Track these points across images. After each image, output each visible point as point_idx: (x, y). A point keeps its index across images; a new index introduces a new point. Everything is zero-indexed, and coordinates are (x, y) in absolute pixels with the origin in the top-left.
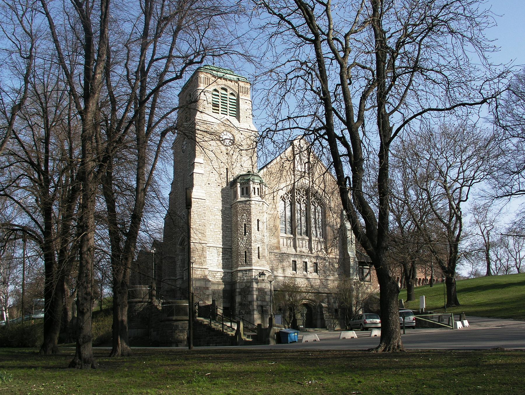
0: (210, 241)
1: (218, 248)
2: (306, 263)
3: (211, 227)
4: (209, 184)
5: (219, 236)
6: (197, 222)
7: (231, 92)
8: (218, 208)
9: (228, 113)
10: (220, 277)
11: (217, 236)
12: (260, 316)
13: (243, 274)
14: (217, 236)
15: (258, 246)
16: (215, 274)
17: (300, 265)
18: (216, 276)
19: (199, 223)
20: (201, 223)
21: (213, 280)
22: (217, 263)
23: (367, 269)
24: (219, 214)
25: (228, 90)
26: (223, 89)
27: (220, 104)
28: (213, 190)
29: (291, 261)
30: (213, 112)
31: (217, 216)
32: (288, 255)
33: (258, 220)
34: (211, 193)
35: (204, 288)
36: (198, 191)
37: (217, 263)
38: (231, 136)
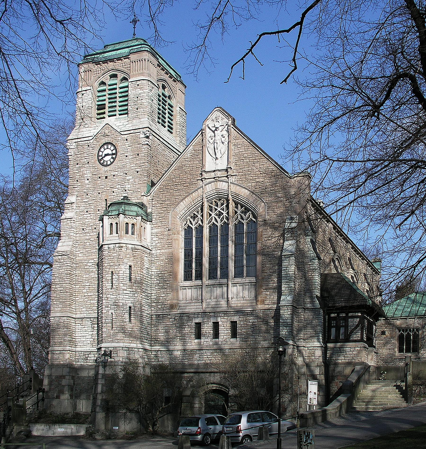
0: (83, 310)
3: (85, 291)
5: (94, 302)
7: (123, 75)
8: (93, 261)
9: (117, 113)
10: (92, 358)
11: (92, 302)
12: (104, 415)
14: (92, 302)
17: (207, 328)
21: (85, 364)
23: (357, 317)
24: (95, 270)
27: (106, 102)
29: (193, 324)
30: (98, 119)
31: (92, 274)
32: (189, 316)
35: (61, 376)
38: (112, 148)
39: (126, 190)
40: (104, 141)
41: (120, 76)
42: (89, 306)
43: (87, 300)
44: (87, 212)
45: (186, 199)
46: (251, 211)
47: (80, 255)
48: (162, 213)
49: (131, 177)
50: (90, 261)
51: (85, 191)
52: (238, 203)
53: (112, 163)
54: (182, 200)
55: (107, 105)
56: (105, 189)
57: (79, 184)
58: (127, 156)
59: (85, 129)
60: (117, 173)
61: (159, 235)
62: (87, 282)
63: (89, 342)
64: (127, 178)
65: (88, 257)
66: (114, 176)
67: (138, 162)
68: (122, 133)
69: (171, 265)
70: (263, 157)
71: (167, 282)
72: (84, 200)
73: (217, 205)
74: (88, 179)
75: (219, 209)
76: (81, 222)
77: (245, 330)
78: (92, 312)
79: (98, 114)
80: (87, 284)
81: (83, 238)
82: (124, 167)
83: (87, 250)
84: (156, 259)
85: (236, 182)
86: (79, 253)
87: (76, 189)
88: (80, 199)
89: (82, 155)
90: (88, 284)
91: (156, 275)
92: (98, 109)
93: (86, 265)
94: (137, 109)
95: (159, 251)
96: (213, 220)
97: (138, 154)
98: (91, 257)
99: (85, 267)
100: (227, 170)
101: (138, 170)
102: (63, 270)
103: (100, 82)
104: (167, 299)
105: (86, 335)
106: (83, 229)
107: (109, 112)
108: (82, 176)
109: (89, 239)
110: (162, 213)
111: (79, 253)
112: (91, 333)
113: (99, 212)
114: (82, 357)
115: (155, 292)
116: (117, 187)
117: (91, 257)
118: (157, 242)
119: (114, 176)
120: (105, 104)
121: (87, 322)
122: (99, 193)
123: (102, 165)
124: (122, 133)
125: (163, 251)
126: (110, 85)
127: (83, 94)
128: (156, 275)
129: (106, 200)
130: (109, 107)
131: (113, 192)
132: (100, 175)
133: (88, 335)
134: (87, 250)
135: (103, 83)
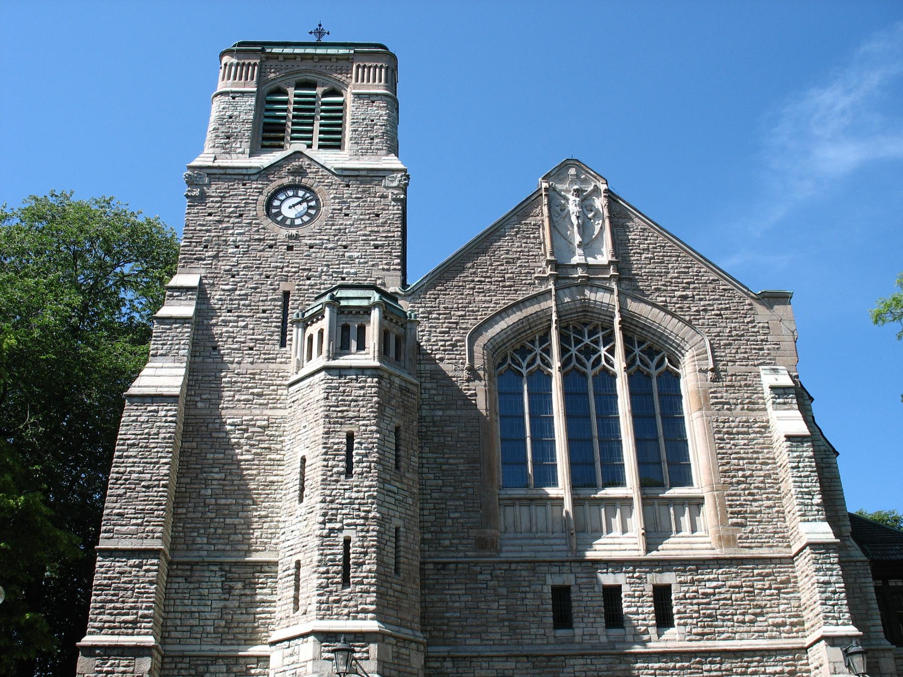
11: (228, 521)
29: (547, 589)
42: (220, 531)
43: (213, 515)
47: (200, 405)
69: (475, 447)
71: (467, 484)
73: (581, 333)
75: (587, 341)
77: (696, 607)
78: (228, 547)
79: (264, 139)
84: (432, 429)
86: (198, 399)
91: (434, 466)
92: (264, 131)
94: (372, 139)
95: (440, 413)
96: (574, 362)
97: (378, 215)
103: (273, 87)
104: (468, 525)
112: (220, 604)
115: (431, 506)
128: (434, 466)
133: (208, 609)
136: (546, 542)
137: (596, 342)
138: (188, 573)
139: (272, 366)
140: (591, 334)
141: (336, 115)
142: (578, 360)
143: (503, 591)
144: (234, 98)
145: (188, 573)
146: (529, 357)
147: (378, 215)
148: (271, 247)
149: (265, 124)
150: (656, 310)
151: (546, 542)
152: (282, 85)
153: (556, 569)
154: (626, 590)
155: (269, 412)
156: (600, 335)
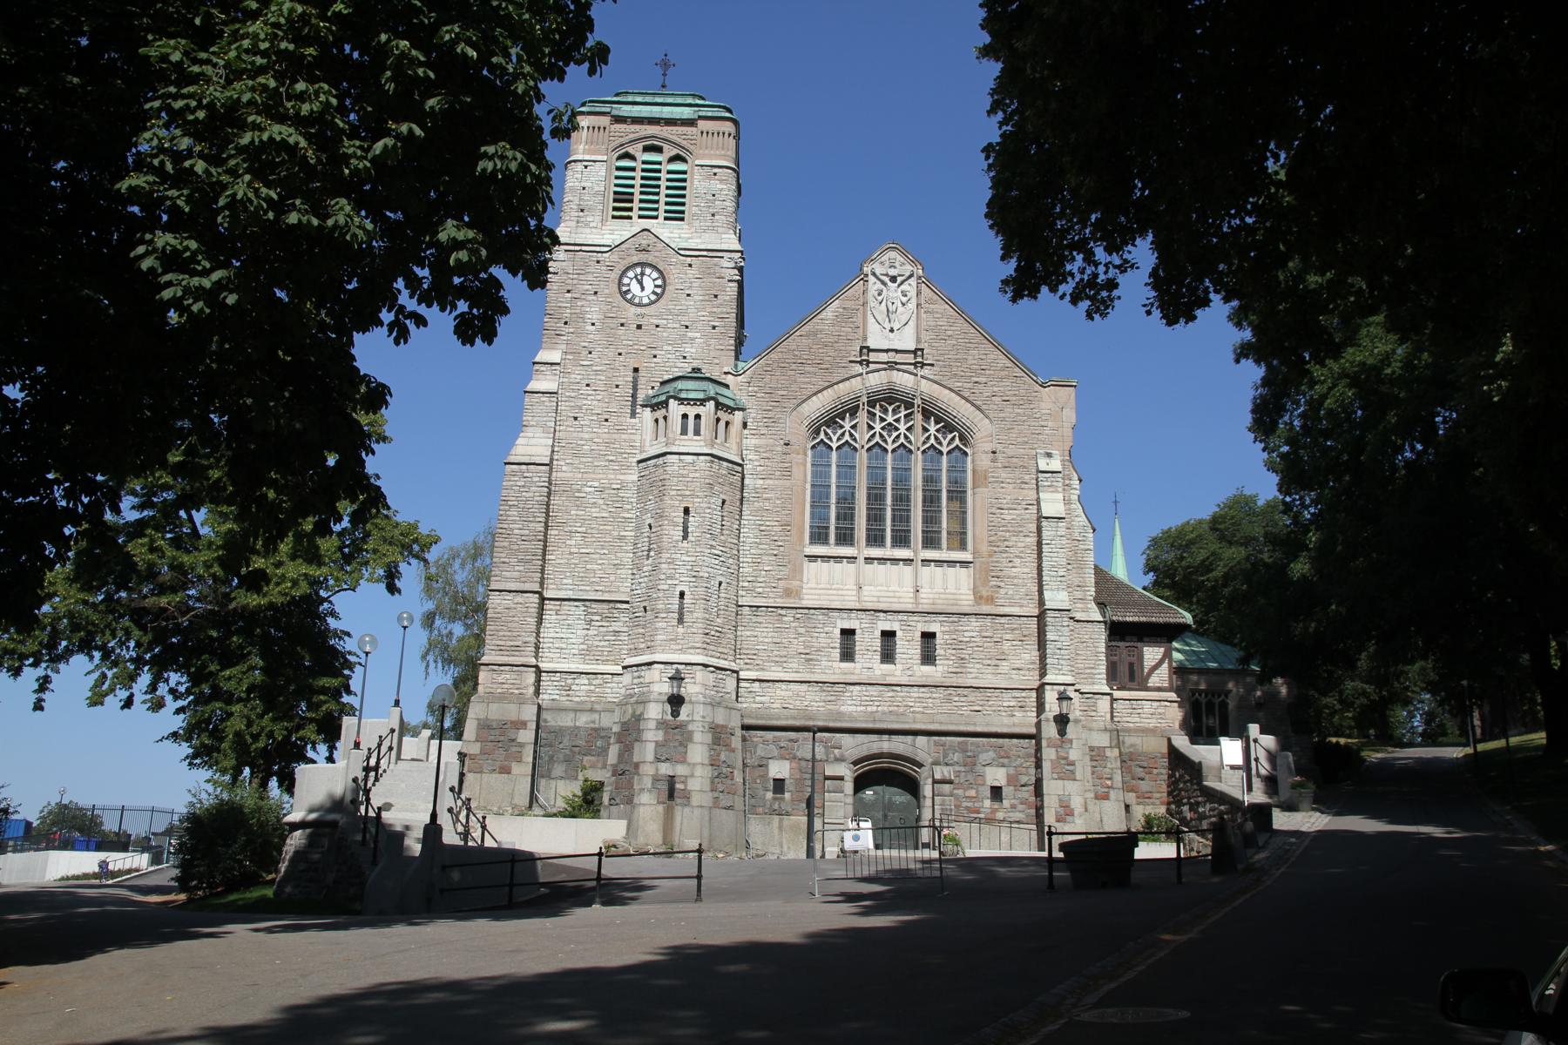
0: (565, 581)
1: (588, 603)
2: (932, 635)
3: (573, 542)
4: (576, 418)
6: (516, 531)
7: (675, 152)
8: (596, 484)
9: (662, 215)
11: (588, 567)
13: (634, 678)
15: (679, 589)
16: (569, 681)
17: (868, 642)
18: (573, 687)
19: (523, 532)
20: (527, 532)
22: (582, 647)
25: (666, 147)
26: (647, 149)
27: (637, 190)
28: (586, 436)
31: (593, 510)
33: (686, 511)
34: (579, 442)
36: (533, 441)
37: (582, 647)
38: (655, 275)
39: (685, 358)
40: (635, 259)
41: (670, 151)
44: (588, 385)
45: (825, 392)
46: (959, 431)
48: (770, 410)
49: (698, 335)
50: (589, 484)
51: (586, 344)
52: (932, 414)
53: (652, 303)
54: (815, 394)
55: (637, 197)
56: (636, 347)
57: (571, 330)
58: (688, 295)
59: (588, 230)
60: (665, 322)
61: (762, 450)
62: (579, 524)
63: (576, 652)
64: (690, 334)
65: (585, 475)
66: (657, 326)
67: (715, 310)
68: (682, 252)
70: (986, 342)
72: (582, 363)
74: (593, 324)
75: (890, 419)
76: (572, 404)
79: (615, 209)
80: (579, 530)
81: (575, 434)
82: (683, 313)
83: (584, 460)
85: (932, 377)
86: (563, 463)
87: (565, 338)
88: (571, 357)
89: (582, 277)
90: (583, 529)
93: (579, 491)
94: (713, 215)
95: (761, 482)
97: (716, 296)
98: (593, 476)
99: (577, 494)
100: (915, 352)
101: (716, 324)
102: (531, 494)
105: (571, 636)
106: (576, 418)
107: (640, 209)
108: (581, 317)
109: (591, 440)
110: (770, 410)
111: (563, 463)
113: (617, 390)
114: (555, 683)
116: (665, 348)
117: (593, 476)
118: (757, 464)
119: (657, 326)
120: (632, 194)
121: (574, 609)
122: (620, 354)
123: (630, 302)
124: (682, 252)
125: (771, 482)
126: (644, 162)
127: (586, 167)
129: (636, 370)
130: (641, 201)
131: (655, 357)
132: (623, 321)
134: (584, 460)
135: (627, 156)
136: (840, 592)
137: (897, 420)
138: (558, 608)
139: (624, 436)
140: (895, 412)
141: (679, 184)
142: (881, 436)
143: (802, 630)
144: (586, 167)
145: (558, 608)
146: (840, 432)
147: (716, 296)
148: (622, 325)
149: (615, 193)
150: (953, 395)
151: (840, 592)
152: (630, 150)
153: (845, 615)
154: (899, 634)
155: (622, 477)
156: (902, 414)
